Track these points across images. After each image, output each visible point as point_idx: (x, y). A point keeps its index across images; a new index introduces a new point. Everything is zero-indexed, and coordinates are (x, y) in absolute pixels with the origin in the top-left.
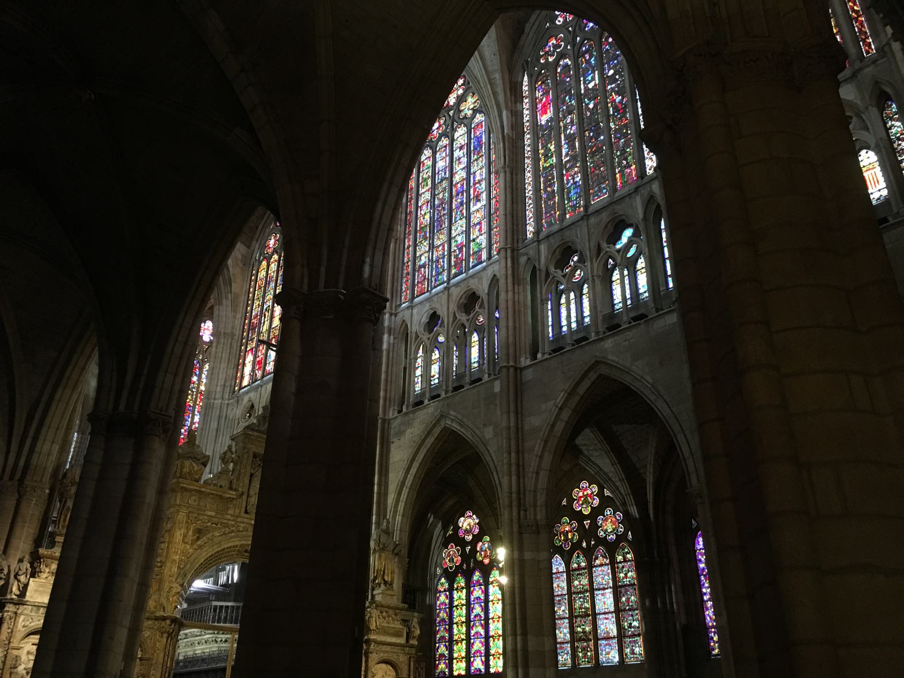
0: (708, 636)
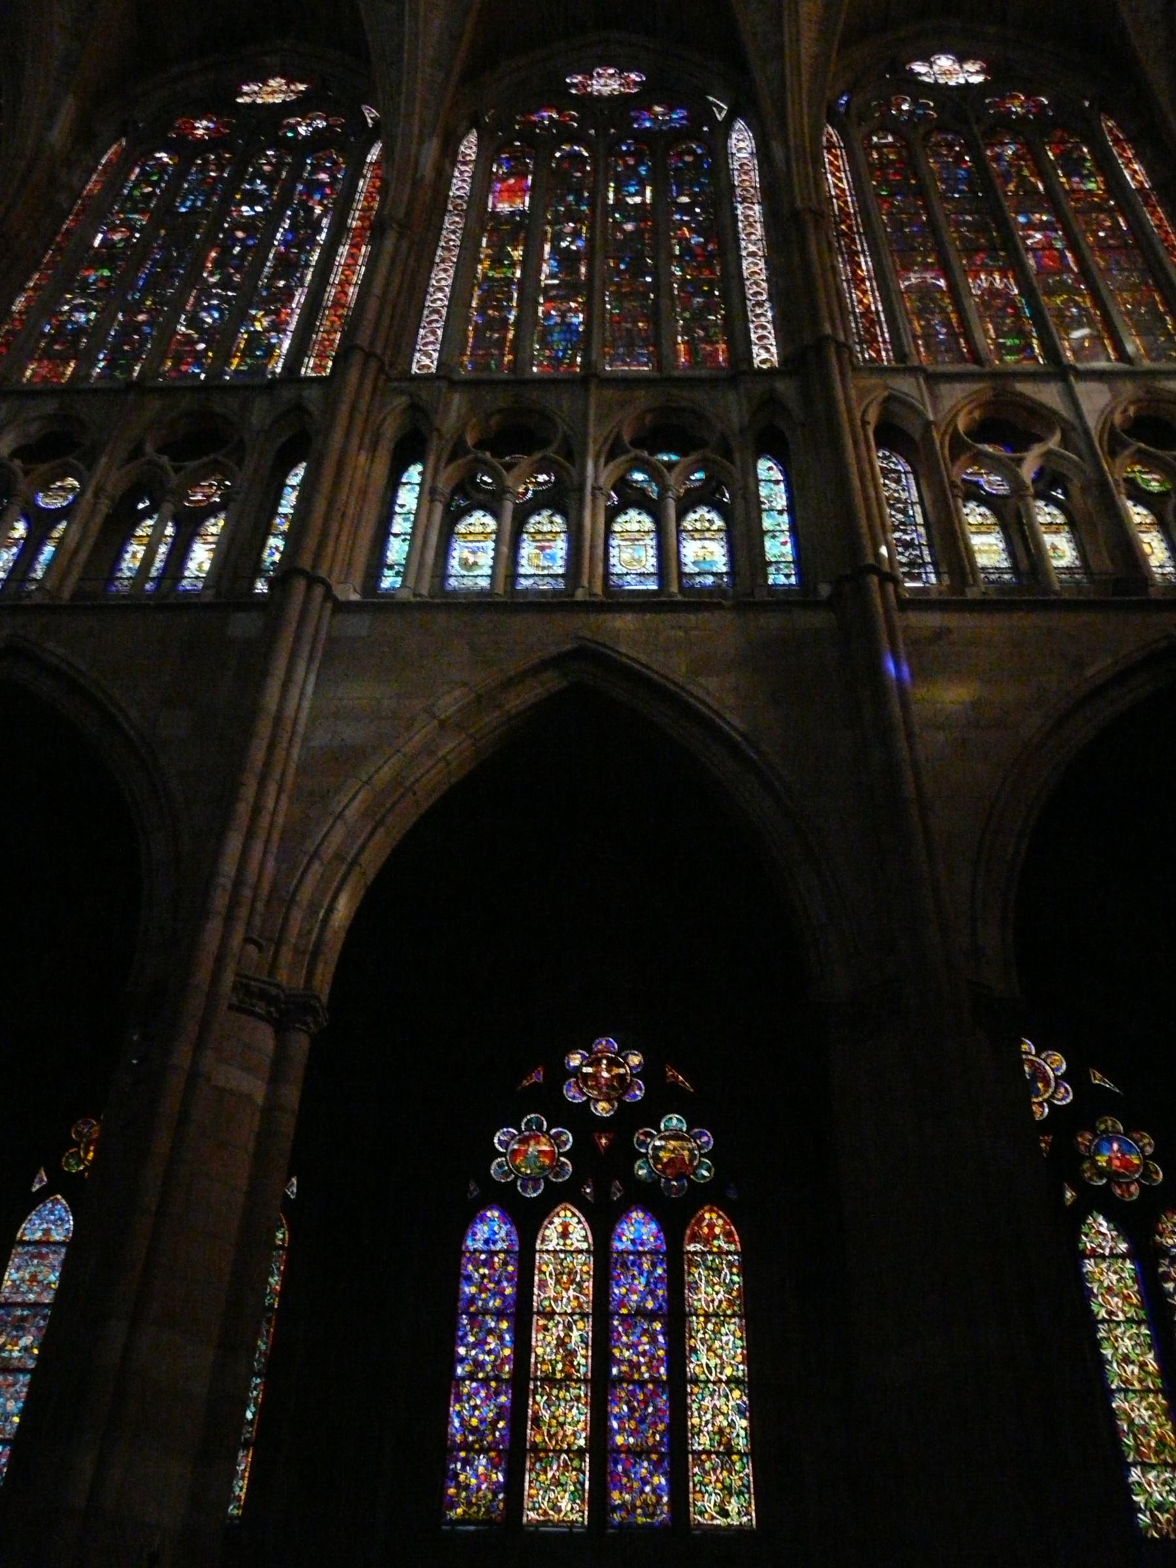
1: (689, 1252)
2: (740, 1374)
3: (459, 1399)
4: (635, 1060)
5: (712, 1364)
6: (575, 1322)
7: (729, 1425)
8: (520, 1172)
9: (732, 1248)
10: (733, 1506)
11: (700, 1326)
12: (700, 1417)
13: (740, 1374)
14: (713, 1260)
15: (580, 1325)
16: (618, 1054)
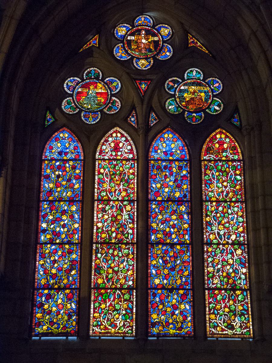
0: (33, 301)
1: (205, 160)
2: (242, 239)
3: (43, 256)
4: (165, 31)
5: (222, 233)
6: (125, 206)
7: (234, 271)
8: (82, 107)
9: (236, 157)
10: (237, 322)
11: (213, 209)
12: (214, 268)
13: (242, 239)
14: (222, 166)
15: (128, 208)
16: (154, 27)
